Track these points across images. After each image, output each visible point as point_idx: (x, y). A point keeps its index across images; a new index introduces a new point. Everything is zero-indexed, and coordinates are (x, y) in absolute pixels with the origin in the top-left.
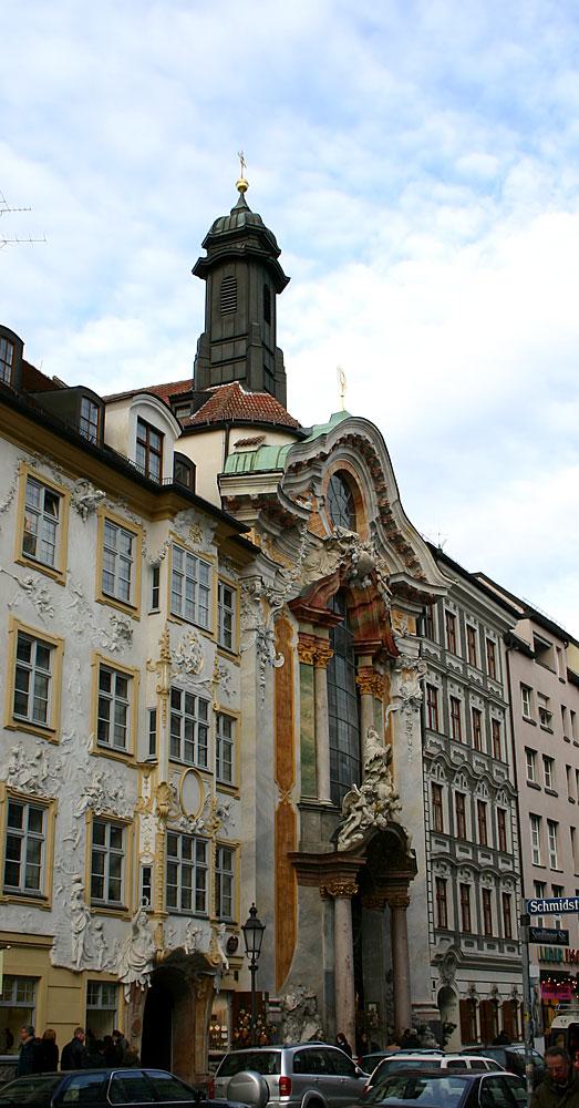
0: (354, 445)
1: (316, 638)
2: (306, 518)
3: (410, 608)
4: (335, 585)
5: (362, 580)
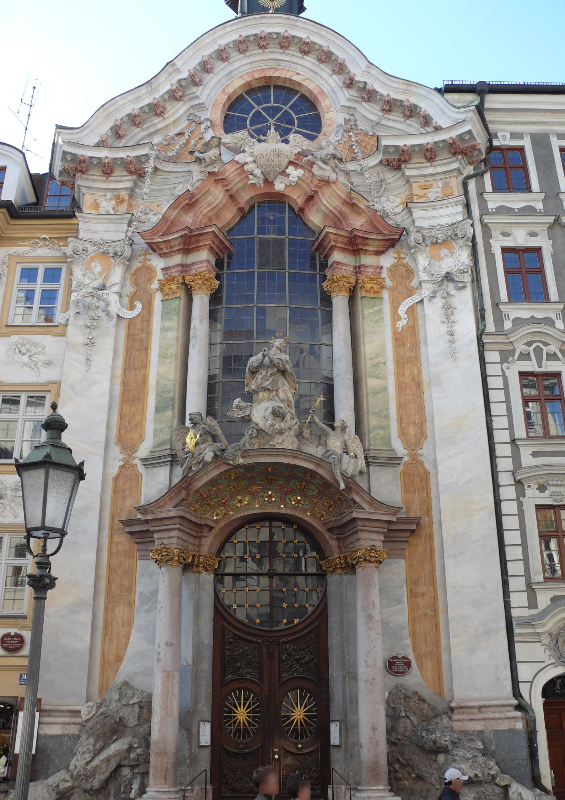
0: (262, 47)
1: (182, 265)
2: (145, 151)
3: (440, 169)
4: (210, 198)
5: (283, 173)
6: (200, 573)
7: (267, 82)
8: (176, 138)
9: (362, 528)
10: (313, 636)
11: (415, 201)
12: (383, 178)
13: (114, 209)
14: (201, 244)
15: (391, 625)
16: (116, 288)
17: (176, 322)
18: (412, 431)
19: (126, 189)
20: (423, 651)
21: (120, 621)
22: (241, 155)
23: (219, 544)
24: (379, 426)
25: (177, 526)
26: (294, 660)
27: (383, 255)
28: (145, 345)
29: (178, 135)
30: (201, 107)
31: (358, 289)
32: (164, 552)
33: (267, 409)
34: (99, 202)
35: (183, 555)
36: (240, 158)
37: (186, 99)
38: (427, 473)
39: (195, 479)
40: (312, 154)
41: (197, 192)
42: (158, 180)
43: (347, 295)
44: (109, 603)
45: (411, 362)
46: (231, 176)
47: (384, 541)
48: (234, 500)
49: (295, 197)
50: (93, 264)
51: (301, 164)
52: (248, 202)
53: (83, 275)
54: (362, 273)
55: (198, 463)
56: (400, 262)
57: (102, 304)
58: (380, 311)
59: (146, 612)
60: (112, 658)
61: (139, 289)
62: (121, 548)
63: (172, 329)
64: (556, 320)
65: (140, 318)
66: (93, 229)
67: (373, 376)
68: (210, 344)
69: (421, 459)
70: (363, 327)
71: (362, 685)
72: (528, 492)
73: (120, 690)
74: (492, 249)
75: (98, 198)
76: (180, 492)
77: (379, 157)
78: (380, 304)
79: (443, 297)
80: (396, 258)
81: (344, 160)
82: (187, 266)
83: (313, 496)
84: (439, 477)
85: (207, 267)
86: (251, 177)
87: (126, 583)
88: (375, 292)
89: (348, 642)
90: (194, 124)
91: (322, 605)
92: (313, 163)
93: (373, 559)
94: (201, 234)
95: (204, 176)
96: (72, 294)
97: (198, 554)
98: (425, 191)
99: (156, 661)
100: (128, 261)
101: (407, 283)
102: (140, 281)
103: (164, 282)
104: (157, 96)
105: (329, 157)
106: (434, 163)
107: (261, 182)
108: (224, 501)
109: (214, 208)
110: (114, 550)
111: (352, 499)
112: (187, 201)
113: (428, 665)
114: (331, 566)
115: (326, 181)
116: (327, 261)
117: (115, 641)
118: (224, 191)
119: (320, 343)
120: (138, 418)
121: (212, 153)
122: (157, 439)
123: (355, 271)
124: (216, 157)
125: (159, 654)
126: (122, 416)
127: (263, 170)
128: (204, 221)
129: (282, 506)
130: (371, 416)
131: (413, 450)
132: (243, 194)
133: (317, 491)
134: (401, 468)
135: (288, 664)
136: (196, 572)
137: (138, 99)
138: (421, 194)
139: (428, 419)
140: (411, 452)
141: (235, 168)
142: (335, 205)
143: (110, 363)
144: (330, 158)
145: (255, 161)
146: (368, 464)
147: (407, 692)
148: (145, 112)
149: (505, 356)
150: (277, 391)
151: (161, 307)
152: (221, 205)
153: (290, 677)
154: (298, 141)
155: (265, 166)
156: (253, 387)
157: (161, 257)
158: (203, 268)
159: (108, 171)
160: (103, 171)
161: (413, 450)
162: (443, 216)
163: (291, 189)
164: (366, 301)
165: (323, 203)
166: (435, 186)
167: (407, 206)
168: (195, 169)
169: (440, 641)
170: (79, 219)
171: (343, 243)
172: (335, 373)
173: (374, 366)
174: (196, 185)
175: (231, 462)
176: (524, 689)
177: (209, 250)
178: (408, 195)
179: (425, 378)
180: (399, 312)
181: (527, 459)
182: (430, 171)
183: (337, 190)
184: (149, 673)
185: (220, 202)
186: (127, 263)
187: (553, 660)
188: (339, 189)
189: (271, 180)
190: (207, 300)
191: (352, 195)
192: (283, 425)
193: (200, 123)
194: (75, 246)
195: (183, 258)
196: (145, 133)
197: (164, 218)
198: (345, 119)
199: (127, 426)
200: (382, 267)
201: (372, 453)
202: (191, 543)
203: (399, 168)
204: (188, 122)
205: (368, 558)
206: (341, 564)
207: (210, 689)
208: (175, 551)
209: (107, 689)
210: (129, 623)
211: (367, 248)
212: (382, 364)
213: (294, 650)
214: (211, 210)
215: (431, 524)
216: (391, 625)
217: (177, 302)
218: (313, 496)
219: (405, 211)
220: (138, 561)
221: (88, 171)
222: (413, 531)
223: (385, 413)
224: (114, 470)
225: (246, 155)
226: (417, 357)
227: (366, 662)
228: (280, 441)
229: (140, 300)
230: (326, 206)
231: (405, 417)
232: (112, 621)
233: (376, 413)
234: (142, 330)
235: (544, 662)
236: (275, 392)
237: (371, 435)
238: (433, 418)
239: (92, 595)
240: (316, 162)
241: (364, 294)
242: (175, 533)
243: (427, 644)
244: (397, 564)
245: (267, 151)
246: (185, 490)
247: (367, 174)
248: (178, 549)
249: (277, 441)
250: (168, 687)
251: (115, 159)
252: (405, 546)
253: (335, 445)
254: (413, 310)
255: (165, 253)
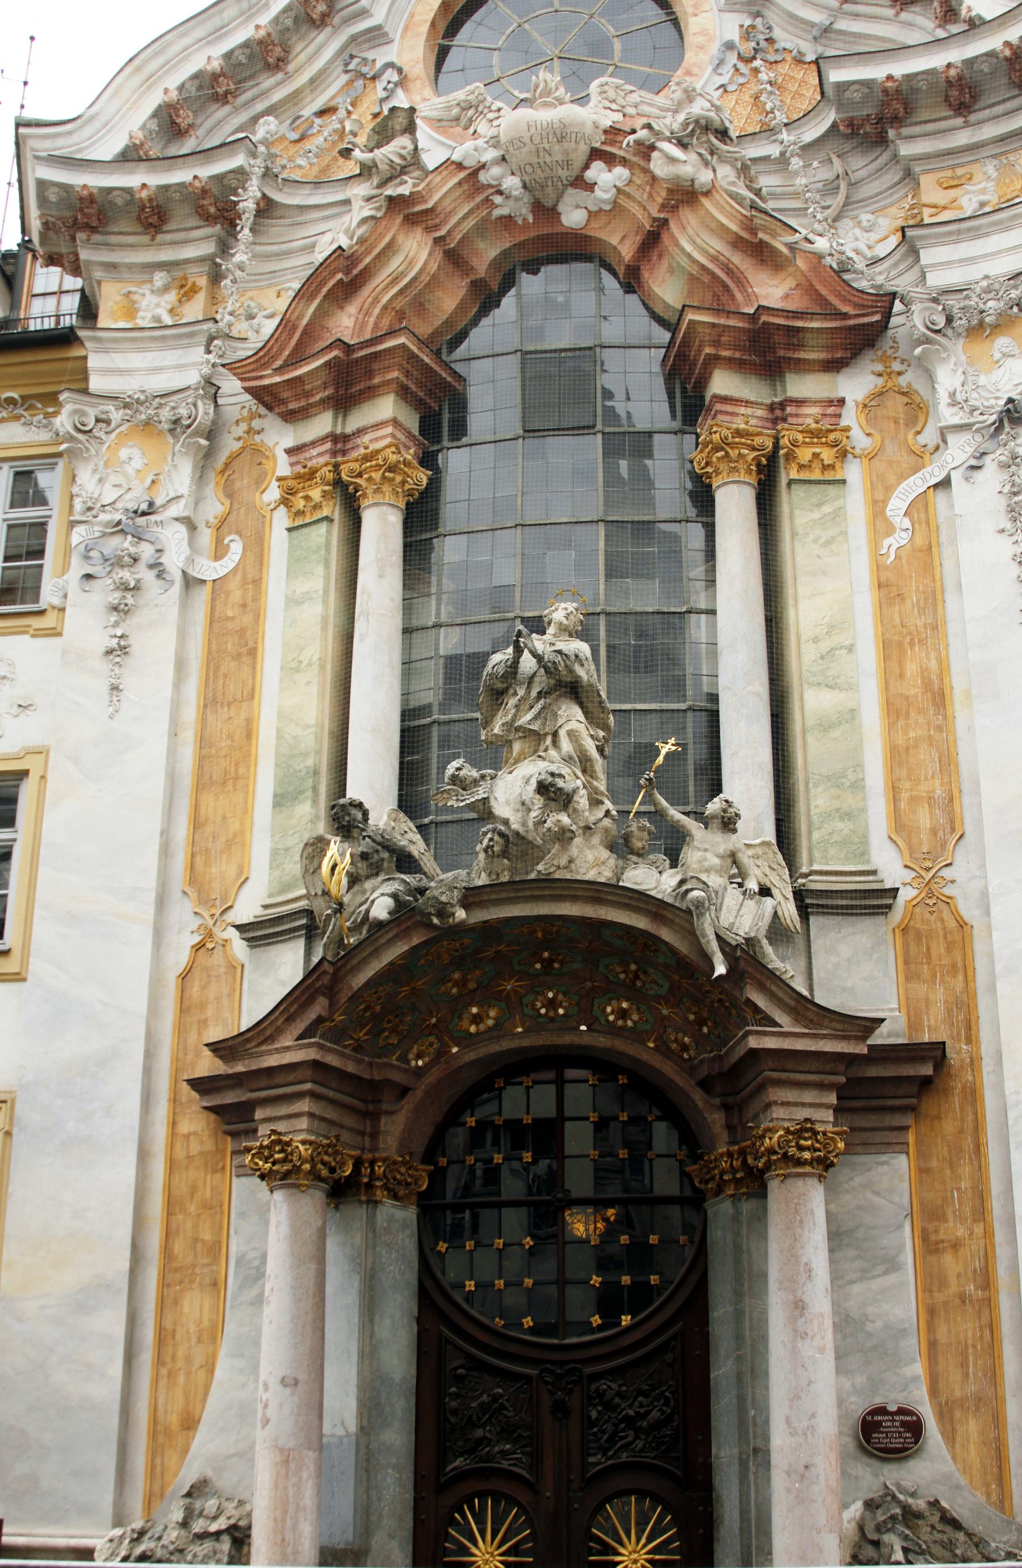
2: (238, 160)
3: (989, 131)
4: (395, 264)
5: (580, 182)
6: (376, 1203)
8: (318, 121)
9: (775, 1075)
10: (669, 1357)
11: (927, 220)
12: (841, 171)
13: (171, 311)
14: (376, 380)
15: (869, 1327)
16: (177, 510)
17: (321, 581)
18: (924, 819)
19: (200, 260)
20: (958, 1394)
21: (192, 1328)
22: (470, 145)
23: (429, 1131)
24: (837, 810)
25: (308, 1086)
26: (621, 1421)
27: (845, 370)
28: (251, 643)
29: (322, 113)
30: (376, 36)
31: (782, 461)
32: (279, 1152)
33: (527, 782)
34: (136, 297)
35: (326, 1158)
36: (465, 150)
37: (337, 20)
38: (962, 925)
39: (349, 967)
40: (649, 126)
41: (363, 249)
42: (276, 229)
43: (753, 480)
44: (169, 1285)
45: (919, 641)
46: (447, 202)
47: (837, 1110)
48: (460, 1017)
49: (614, 241)
50: (124, 453)
51: (621, 153)
52: (495, 264)
53: (100, 480)
54: (790, 420)
55: (355, 928)
56: (890, 384)
57: (146, 551)
58: (838, 515)
59: (252, 1304)
60: (174, 1419)
61: (236, 506)
62: (195, 1148)
63: (311, 598)
65: (239, 576)
66: (122, 365)
67: (819, 684)
68: (407, 631)
69: (947, 891)
70: (794, 558)
71: (779, 1482)
73: (188, 1500)
75: (133, 289)
76: (311, 1000)
77: (829, 117)
78: (837, 498)
79: (1004, 466)
80: (880, 375)
81: (734, 133)
82: (346, 438)
83: (658, 998)
84: (995, 935)
85: (393, 435)
86: (498, 199)
87: (207, 1236)
88: (825, 468)
89: (753, 1371)
90: (360, 82)
91: (694, 1277)
92: (653, 148)
93: (807, 1155)
94: (376, 355)
95: (378, 209)
96: (75, 530)
97: (370, 1156)
98: (953, 193)
99: (259, 1424)
100: (207, 439)
101: (910, 436)
102: (238, 485)
103: (291, 483)
104: (265, 19)
105: (691, 128)
106: (973, 118)
107: (524, 211)
108: (434, 1020)
109: (407, 286)
110: (180, 1153)
111: (749, 1002)
112: (340, 276)
113: (972, 1427)
114: (713, 1178)
115: (687, 193)
116: (702, 398)
117: (181, 1379)
118: (430, 242)
119: (684, 609)
120: (235, 826)
121: (397, 147)
122: (277, 873)
123: (770, 416)
124: (405, 159)
125: (266, 1406)
126: (197, 823)
127: (527, 178)
128: (385, 323)
129: (583, 1028)
130: (816, 786)
131: (928, 869)
132: (481, 245)
133: (666, 986)
134: (898, 914)
135: (604, 1432)
136: (368, 1202)
137: (219, 33)
138: (942, 202)
139: (965, 787)
140: (923, 873)
141: (455, 180)
142: (712, 251)
143: (168, 692)
144: (693, 131)
145: (504, 159)
146: (804, 911)
147: (910, 1500)
148: (240, 64)
150: (555, 735)
151: (286, 545)
152: (425, 278)
153: (610, 1462)
154: (612, 94)
155: (529, 169)
156: (497, 730)
157: (286, 421)
158: (379, 441)
159: (153, 220)
160: (139, 218)
161: (928, 869)
162: (999, 252)
163: (603, 220)
164: (798, 491)
165: (683, 250)
166: (976, 178)
167: (904, 236)
168: (360, 190)
169: (1001, 1365)
170: (88, 344)
171: (735, 348)
172: (723, 682)
173: (822, 657)
174: (359, 232)
175: (435, 921)
177: (397, 393)
178: (912, 207)
179: (957, 682)
180: (888, 513)
182: (962, 138)
183: (715, 212)
184: (247, 1456)
185: (421, 271)
186: (204, 442)
188: (722, 210)
189: (548, 203)
190: (395, 519)
191: (755, 221)
192: (565, 819)
193: (374, 78)
194: (75, 412)
195: (335, 418)
196: (244, 117)
197: (286, 325)
198: (742, 26)
199: (210, 845)
200: (842, 402)
201: (817, 883)
202: (351, 1130)
203: (881, 141)
204: (344, 78)
205: (792, 1151)
206: (733, 1170)
207: (409, 1496)
208: (301, 1148)
209: (162, 1495)
210: (213, 1334)
211: (802, 355)
212: (844, 652)
213: (619, 1394)
214: (401, 292)
215: (975, 1062)
216: (869, 1327)
217: (323, 527)
218: (658, 998)
219: (902, 250)
220: (234, 1178)
221: (105, 225)
222: (926, 1083)
223: (852, 777)
224: (179, 956)
225: (480, 142)
226: (937, 627)
227: (788, 1421)
228: (563, 862)
229: (239, 533)
230: (689, 256)
231: (907, 785)
232: (174, 1331)
233: (829, 778)
234: (244, 606)
236: (549, 740)
237: (816, 836)
238: (978, 783)
239: (126, 1265)
240: (659, 144)
241: (794, 475)
242: (304, 1105)
244: (885, 1168)
245: (533, 130)
246: (324, 994)
247: (796, 163)
248: (311, 1143)
249: (555, 863)
250: (286, 1488)
251: (166, 188)
252: (908, 1120)
253: (706, 864)
254: (926, 506)
255: (293, 412)
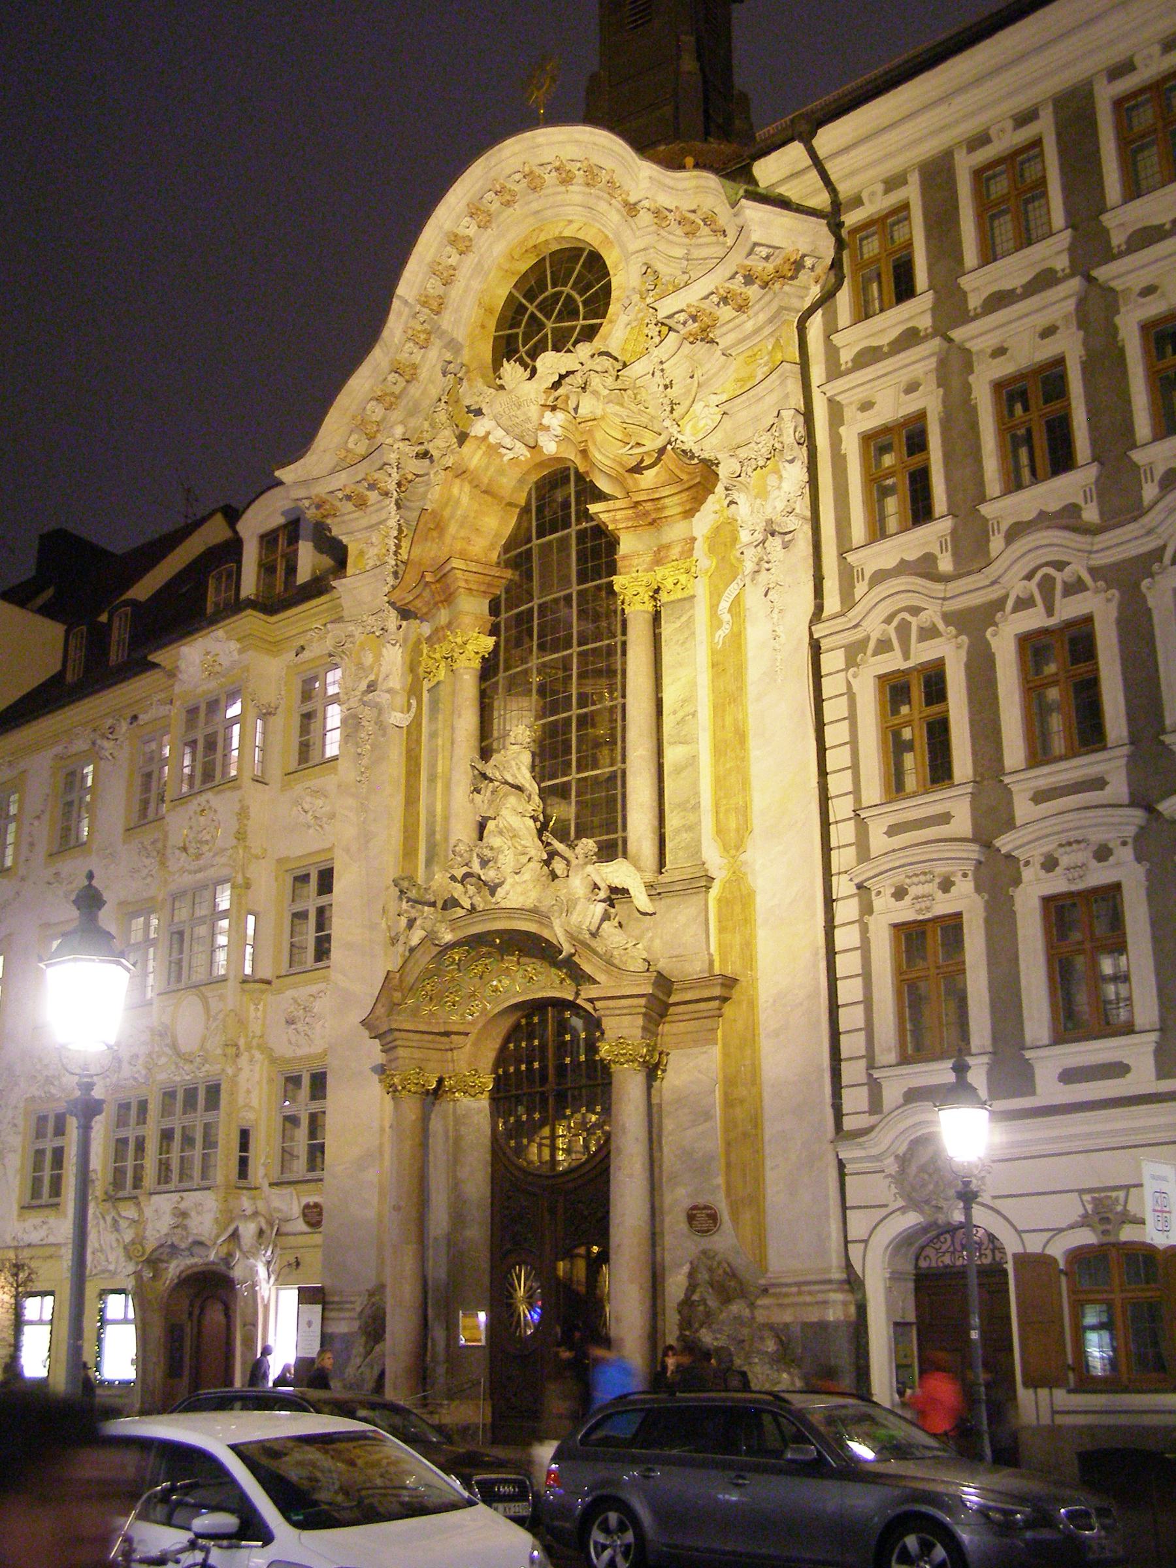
7: (538, 255)
64: (940, 556)
72: (878, 903)
74: (843, 447)
149: (854, 653)
171: (628, 519)
176: (855, 1251)
181: (878, 841)
187: (900, 1203)
211: (667, 513)
215: (754, 980)
223: (693, 802)
233: (679, 805)
235: (886, 1206)
243: (745, 1182)
